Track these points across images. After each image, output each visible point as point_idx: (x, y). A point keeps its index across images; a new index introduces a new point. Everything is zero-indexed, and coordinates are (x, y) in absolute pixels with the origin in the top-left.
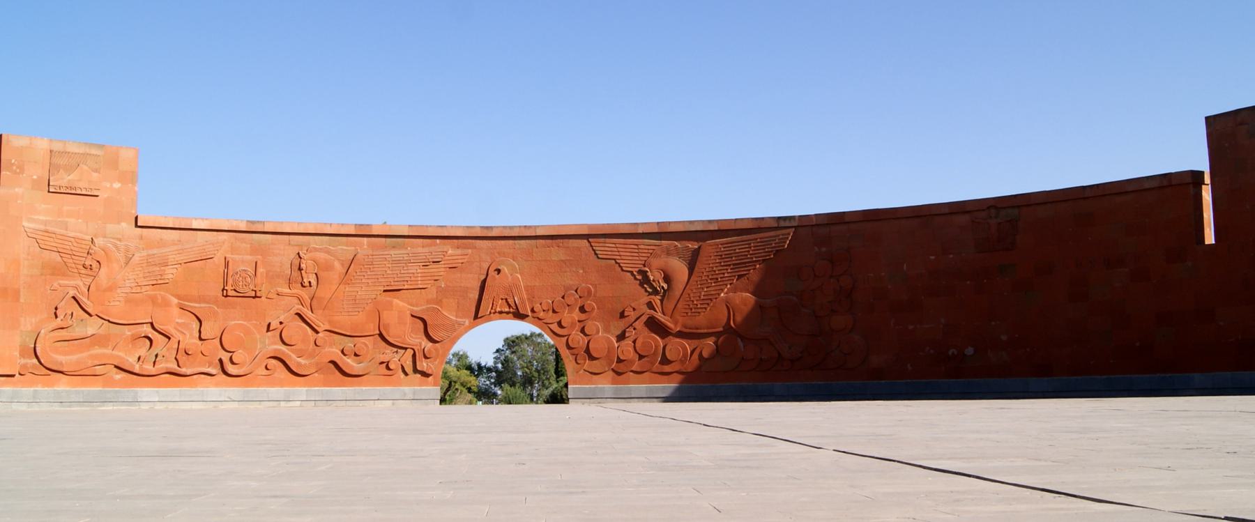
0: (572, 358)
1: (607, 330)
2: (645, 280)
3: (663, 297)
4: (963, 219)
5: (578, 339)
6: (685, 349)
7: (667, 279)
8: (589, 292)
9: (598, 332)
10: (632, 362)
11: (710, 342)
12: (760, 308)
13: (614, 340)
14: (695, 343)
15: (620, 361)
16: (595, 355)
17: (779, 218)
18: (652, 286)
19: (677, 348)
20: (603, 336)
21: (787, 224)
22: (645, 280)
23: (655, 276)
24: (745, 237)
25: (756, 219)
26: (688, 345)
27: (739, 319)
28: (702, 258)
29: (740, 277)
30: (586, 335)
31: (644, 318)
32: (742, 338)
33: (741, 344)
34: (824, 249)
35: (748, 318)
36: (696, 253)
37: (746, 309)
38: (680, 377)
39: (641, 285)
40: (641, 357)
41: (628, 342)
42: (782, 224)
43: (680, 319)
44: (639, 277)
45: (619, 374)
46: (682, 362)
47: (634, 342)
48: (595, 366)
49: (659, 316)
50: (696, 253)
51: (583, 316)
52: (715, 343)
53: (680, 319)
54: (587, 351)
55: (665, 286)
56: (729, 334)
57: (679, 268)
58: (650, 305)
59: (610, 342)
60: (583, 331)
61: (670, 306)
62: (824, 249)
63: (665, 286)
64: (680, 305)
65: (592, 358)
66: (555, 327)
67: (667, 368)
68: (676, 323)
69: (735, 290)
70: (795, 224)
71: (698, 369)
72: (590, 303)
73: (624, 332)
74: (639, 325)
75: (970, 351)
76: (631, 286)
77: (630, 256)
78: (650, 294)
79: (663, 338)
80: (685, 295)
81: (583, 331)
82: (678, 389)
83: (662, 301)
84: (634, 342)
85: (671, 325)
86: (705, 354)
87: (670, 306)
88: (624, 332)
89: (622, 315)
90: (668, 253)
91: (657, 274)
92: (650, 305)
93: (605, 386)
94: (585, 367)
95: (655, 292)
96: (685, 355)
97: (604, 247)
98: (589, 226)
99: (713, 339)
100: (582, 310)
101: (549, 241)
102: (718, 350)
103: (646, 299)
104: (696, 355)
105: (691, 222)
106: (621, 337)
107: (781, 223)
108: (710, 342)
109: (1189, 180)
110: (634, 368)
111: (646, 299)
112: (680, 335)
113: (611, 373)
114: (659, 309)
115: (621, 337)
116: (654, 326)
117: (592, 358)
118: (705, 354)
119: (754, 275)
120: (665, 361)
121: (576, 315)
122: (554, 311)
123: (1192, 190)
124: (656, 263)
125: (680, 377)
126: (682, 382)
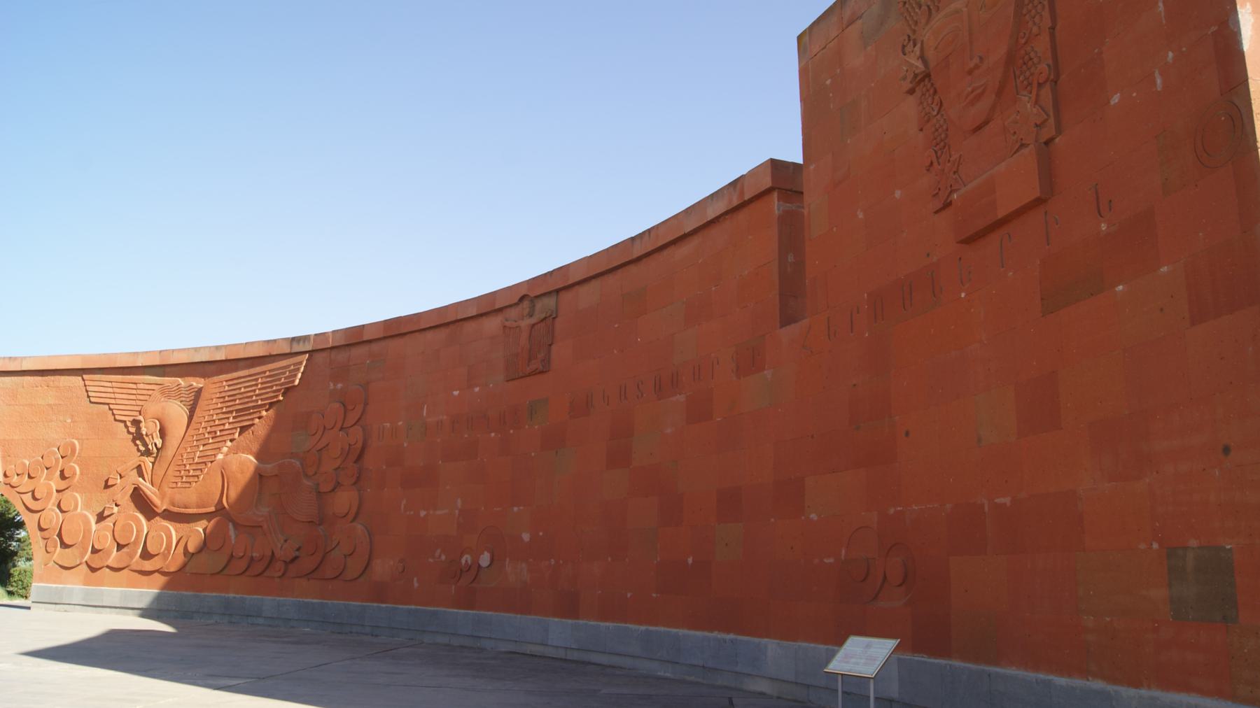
0: (42, 543)
1: (87, 506)
2: (138, 436)
4: (492, 325)
10: (109, 553)
11: (200, 528)
12: (259, 477)
13: (93, 520)
15: (95, 551)
16: (67, 540)
17: (294, 340)
18: (145, 445)
22: (138, 436)
23: (149, 427)
24: (258, 369)
25: (268, 342)
27: (234, 493)
28: (202, 403)
29: (243, 429)
30: (62, 512)
32: (236, 526)
33: (232, 532)
34: (339, 386)
39: (134, 441)
41: (109, 523)
43: (169, 491)
44: (133, 430)
45: (93, 570)
48: (68, 557)
49: (146, 487)
51: (63, 485)
52: (205, 530)
53: (169, 491)
54: (60, 535)
59: (87, 522)
61: (160, 472)
62: (339, 386)
63: (159, 442)
64: (170, 472)
65: (65, 545)
66: (28, 498)
67: (148, 565)
68: (162, 498)
70: (308, 347)
74: (125, 499)
75: (485, 560)
79: (149, 519)
81: (59, 506)
82: (158, 598)
83: (153, 463)
86: (191, 549)
90: (167, 393)
91: (151, 424)
94: (55, 557)
95: (147, 453)
98: (84, 357)
99: (204, 523)
100: (63, 477)
101: (38, 379)
103: (135, 459)
105: (196, 350)
106: (101, 517)
107: (294, 348)
108: (200, 528)
109: (767, 182)
110: (110, 562)
112: (169, 515)
113: (84, 567)
117: (65, 545)
119: (261, 427)
120: (146, 555)
122: (30, 477)
123: (775, 205)
124: (153, 408)
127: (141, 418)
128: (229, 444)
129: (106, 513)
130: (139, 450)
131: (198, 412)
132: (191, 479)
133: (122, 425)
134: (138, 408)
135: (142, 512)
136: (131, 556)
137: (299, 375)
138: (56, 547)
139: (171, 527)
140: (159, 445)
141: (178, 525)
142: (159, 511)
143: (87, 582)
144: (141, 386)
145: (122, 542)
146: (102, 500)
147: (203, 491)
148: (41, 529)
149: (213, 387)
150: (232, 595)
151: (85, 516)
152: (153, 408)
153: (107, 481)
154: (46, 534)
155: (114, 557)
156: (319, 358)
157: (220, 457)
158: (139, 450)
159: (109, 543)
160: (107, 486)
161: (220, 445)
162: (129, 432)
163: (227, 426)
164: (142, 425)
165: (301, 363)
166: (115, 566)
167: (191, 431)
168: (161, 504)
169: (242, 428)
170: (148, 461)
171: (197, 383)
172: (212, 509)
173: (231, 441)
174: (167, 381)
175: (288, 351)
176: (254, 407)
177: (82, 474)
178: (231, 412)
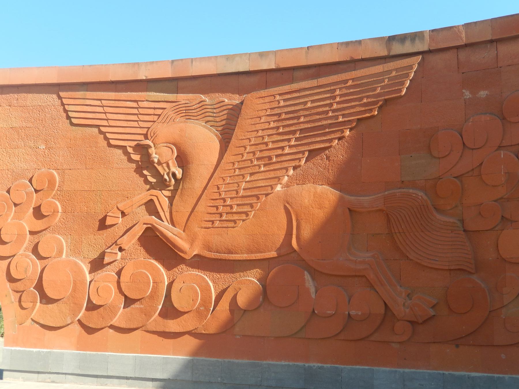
1: (76, 250)
2: (145, 163)
3: (174, 192)
5: (27, 265)
6: (206, 289)
7: (183, 160)
8: (52, 182)
9: (60, 253)
10: (113, 311)
12: (348, 214)
13: (86, 268)
14: (225, 279)
15: (92, 307)
16: (50, 293)
17: (392, 39)
19: (193, 287)
20: (68, 260)
21: (408, 48)
22: (145, 163)
23: (162, 154)
24: (323, 81)
25: (347, 44)
26: (212, 284)
27: (307, 232)
28: (245, 122)
29: (313, 153)
30: (40, 258)
31: (139, 231)
32: (315, 273)
34: (483, 94)
35: (324, 230)
36: (235, 112)
37: (320, 215)
38: (191, 343)
39: (139, 170)
40: (129, 302)
41: (110, 272)
42: (398, 49)
43: (201, 233)
44: (136, 157)
45: (90, 330)
46: (200, 314)
47: (119, 273)
50: (235, 112)
51: (39, 225)
53: (201, 233)
54: (39, 287)
55: (179, 173)
56: (286, 266)
57: (204, 140)
58: (151, 207)
60: (35, 250)
62: (483, 94)
63: (179, 173)
64: (200, 208)
65: (46, 299)
67: (173, 325)
68: (192, 241)
69: (302, 180)
70: (424, 47)
71: (228, 328)
72: (54, 204)
73: (103, 255)
74: (131, 242)
76: (121, 171)
77: (122, 117)
78: (153, 187)
79: (169, 267)
80: (212, 189)
81: (35, 250)
83: (171, 199)
84: (119, 273)
85: (182, 243)
86: (242, 301)
87: (183, 207)
88: (103, 255)
89: (103, 225)
90: (187, 113)
92: (151, 207)
93: (65, 351)
95: (162, 184)
96: (205, 302)
97: (79, 103)
100: (38, 213)
102: (265, 294)
103: (144, 195)
104: (225, 304)
105: (229, 58)
106: (98, 264)
107: (393, 49)
108: (252, 279)
110: (115, 322)
111: (144, 195)
112: (201, 263)
113: (77, 328)
114: (165, 214)
115: (98, 264)
116: (155, 244)
117: (46, 299)
118: (242, 301)
119: (339, 151)
120: (170, 311)
121: (28, 222)
124: (165, 131)
125: (191, 343)
126: (196, 353)
127: (149, 142)
128: (291, 172)
129: (107, 260)
130: (146, 181)
131: (238, 133)
132: (236, 217)
133: (120, 152)
134: (144, 131)
135: (156, 259)
136: (148, 315)
137: (408, 83)
138: (34, 302)
139: (207, 278)
140: (179, 175)
141: (217, 275)
142: (187, 257)
143: (81, 346)
144: (145, 104)
145: (132, 295)
146: (95, 243)
147: (262, 230)
148: (11, 279)
149: (259, 105)
150: (316, 365)
151: (76, 264)
152: (165, 131)
153: (104, 219)
154: (19, 286)
155: (120, 316)
156: (437, 60)
157: (279, 188)
158: (146, 181)
159: (110, 295)
160: (103, 225)
161: (279, 173)
162: (130, 160)
163: (287, 150)
164: (152, 151)
165: (411, 67)
166: (123, 325)
167: (228, 157)
168: (189, 249)
169: (310, 151)
170: (162, 197)
171: (231, 100)
172: (273, 254)
173: (295, 168)
174: (182, 97)
175: (384, 53)
176: (330, 126)
177: (64, 212)
178: (294, 132)
